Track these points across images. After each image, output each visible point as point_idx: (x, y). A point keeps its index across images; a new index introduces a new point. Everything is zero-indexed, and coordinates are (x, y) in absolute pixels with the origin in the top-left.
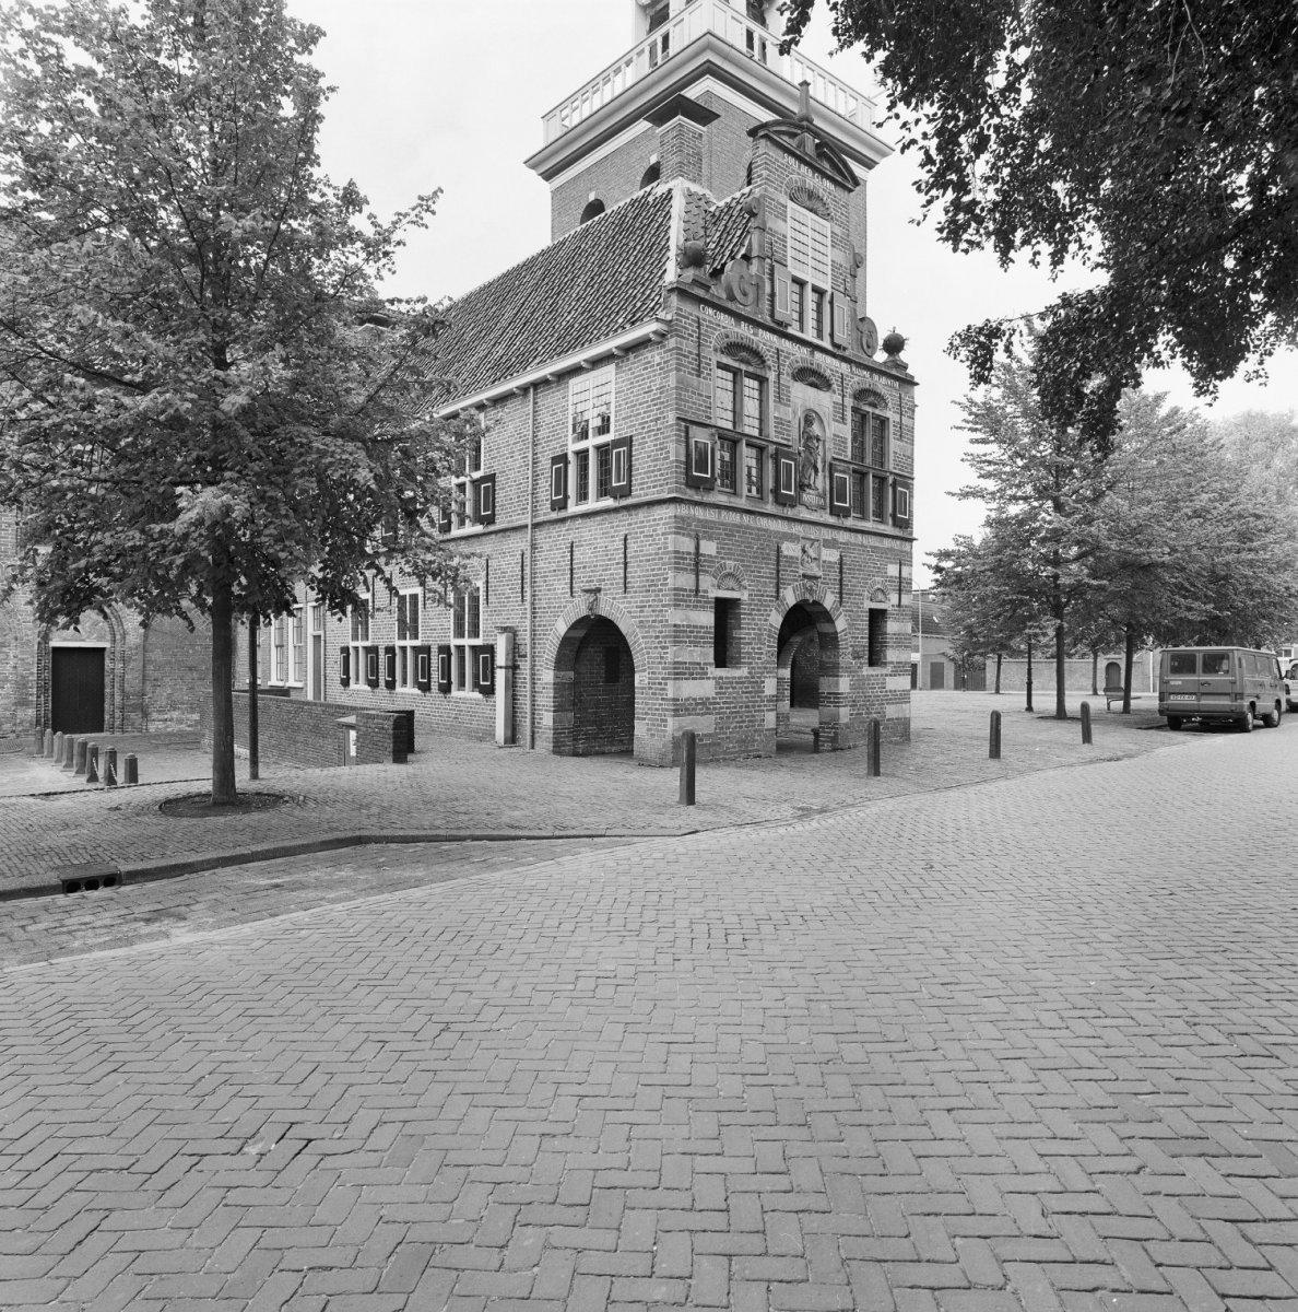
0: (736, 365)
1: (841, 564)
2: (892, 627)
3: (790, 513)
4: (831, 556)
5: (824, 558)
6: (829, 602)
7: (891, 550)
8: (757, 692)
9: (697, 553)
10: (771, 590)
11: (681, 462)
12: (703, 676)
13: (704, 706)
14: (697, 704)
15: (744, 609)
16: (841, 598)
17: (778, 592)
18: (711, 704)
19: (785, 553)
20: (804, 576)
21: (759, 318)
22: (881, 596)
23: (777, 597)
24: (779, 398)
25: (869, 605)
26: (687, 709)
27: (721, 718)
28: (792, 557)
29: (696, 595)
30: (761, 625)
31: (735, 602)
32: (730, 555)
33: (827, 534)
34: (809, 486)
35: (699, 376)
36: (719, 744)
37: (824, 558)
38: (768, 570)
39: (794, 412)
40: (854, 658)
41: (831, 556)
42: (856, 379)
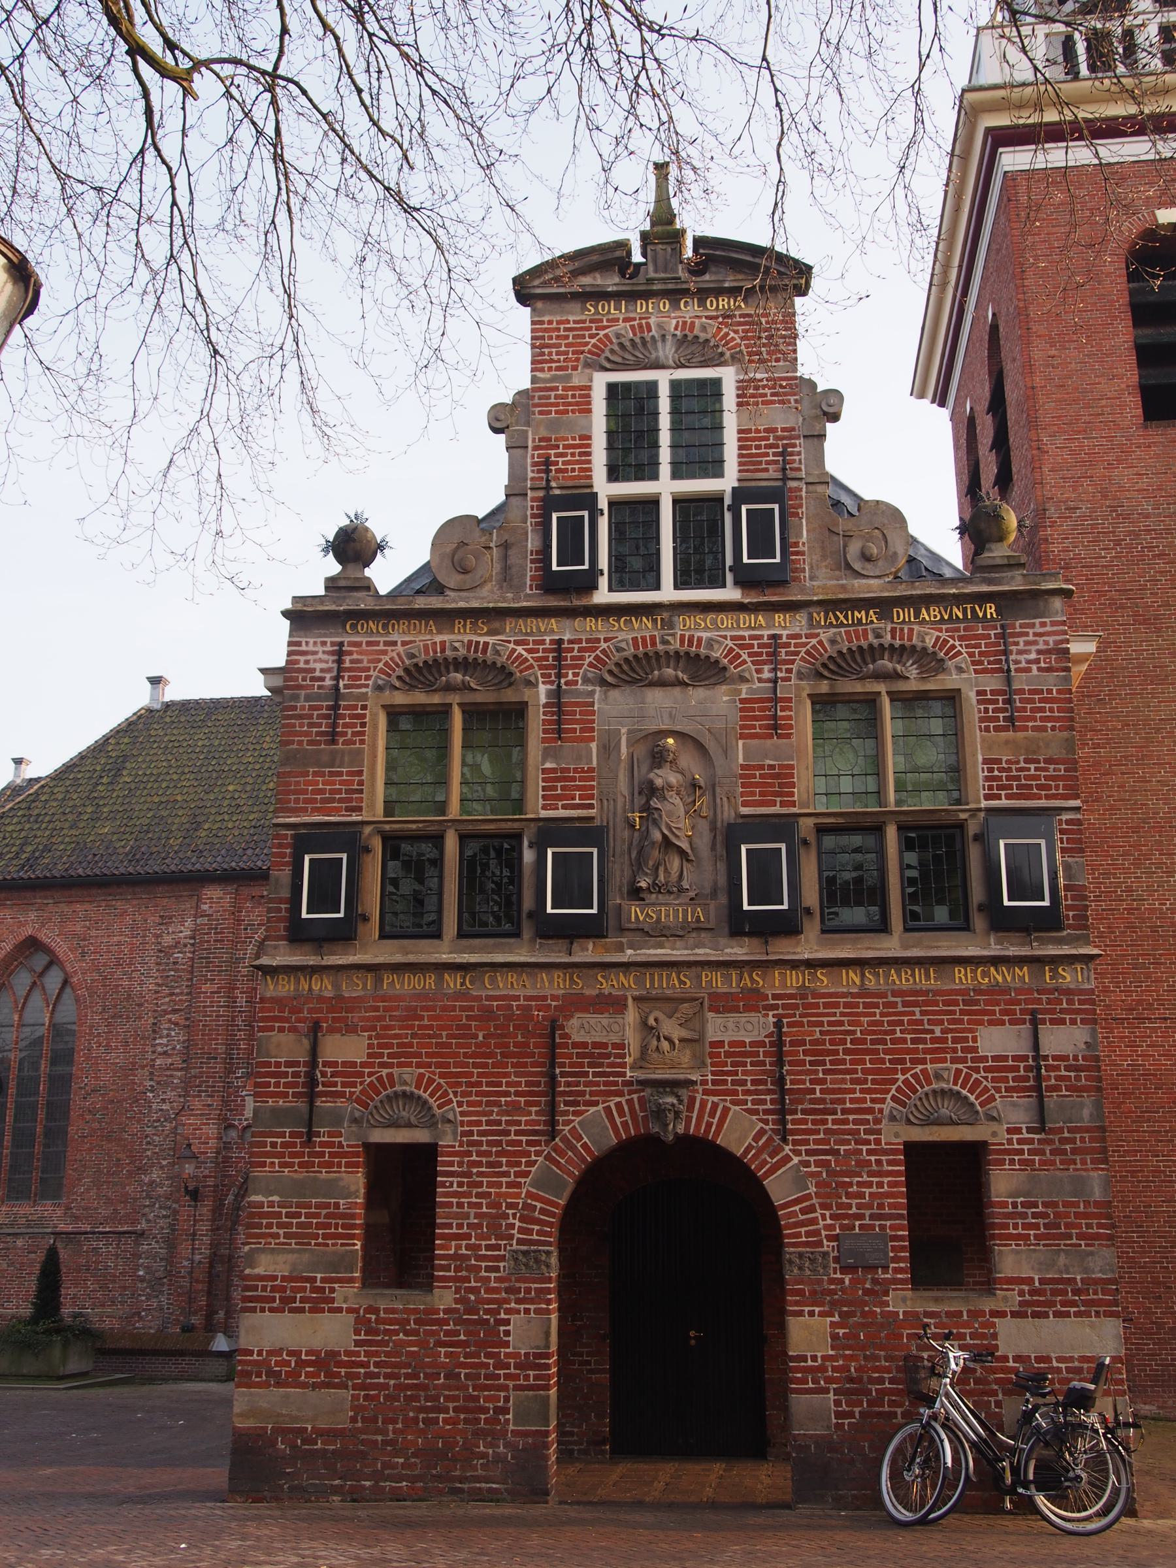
0: (436, 699)
1: (779, 1043)
2: (1003, 1184)
3: (587, 952)
4: (752, 1028)
5: (712, 1034)
6: (740, 1132)
7: (996, 990)
8: (482, 1344)
9: (313, 1063)
10: (533, 1116)
11: (281, 901)
12: (321, 1303)
13: (325, 1367)
14: (301, 1364)
15: (447, 1164)
16: (782, 1112)
17: (553, 1123)
18: (341, 1364)
19: (577, 1038)
20: (640, 1082)
21: (509, 601)
22: (946, 1109)
23: (553, 1134)
24: (557, 730)
25: (894, 1135)
26: (271, 1373)
27: (366, 1397)
28: (596, 1045)
29: (309, 1142)
30: (506, 1203)
31: (427, 1154)
32: (404, 1055)
33: (717, 982)
34: (655, 888)
35: (334, 742)
36: (363, 1455)
37: (712, 1034)
38: (516, 1082)
39: (608, 749)
40: (845, 1270)
41: (752, 1028)
42: (825, 635)
